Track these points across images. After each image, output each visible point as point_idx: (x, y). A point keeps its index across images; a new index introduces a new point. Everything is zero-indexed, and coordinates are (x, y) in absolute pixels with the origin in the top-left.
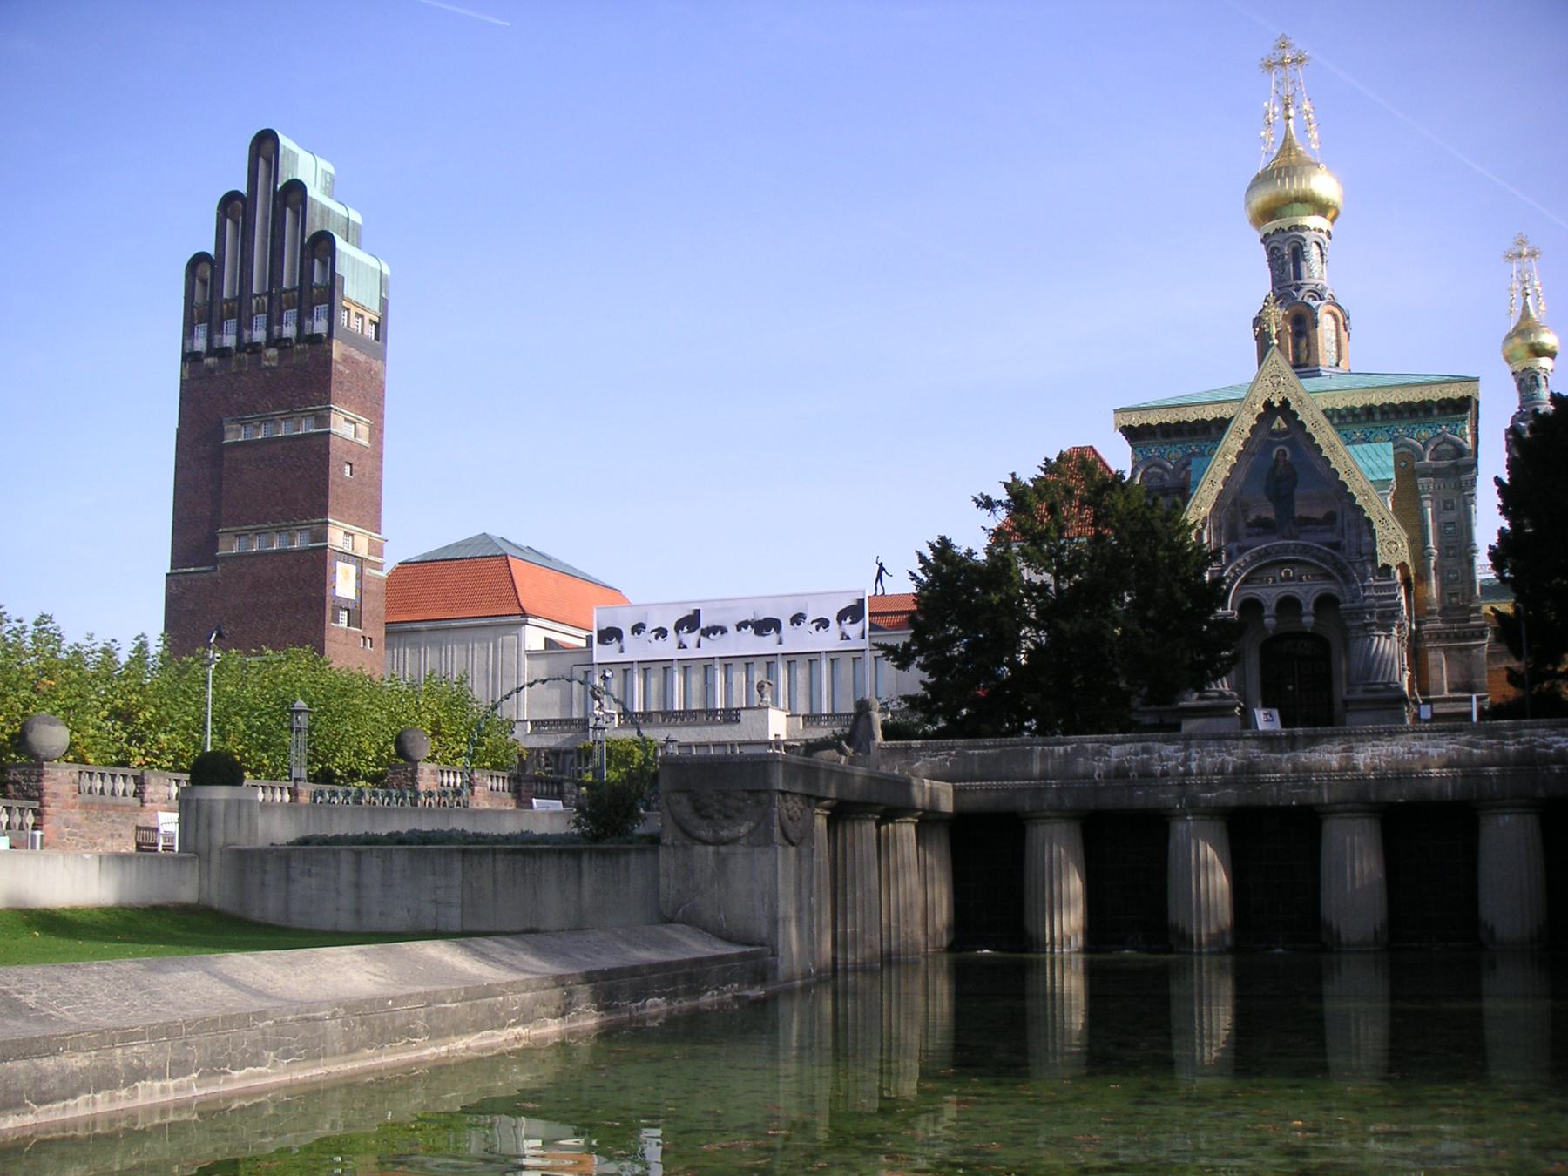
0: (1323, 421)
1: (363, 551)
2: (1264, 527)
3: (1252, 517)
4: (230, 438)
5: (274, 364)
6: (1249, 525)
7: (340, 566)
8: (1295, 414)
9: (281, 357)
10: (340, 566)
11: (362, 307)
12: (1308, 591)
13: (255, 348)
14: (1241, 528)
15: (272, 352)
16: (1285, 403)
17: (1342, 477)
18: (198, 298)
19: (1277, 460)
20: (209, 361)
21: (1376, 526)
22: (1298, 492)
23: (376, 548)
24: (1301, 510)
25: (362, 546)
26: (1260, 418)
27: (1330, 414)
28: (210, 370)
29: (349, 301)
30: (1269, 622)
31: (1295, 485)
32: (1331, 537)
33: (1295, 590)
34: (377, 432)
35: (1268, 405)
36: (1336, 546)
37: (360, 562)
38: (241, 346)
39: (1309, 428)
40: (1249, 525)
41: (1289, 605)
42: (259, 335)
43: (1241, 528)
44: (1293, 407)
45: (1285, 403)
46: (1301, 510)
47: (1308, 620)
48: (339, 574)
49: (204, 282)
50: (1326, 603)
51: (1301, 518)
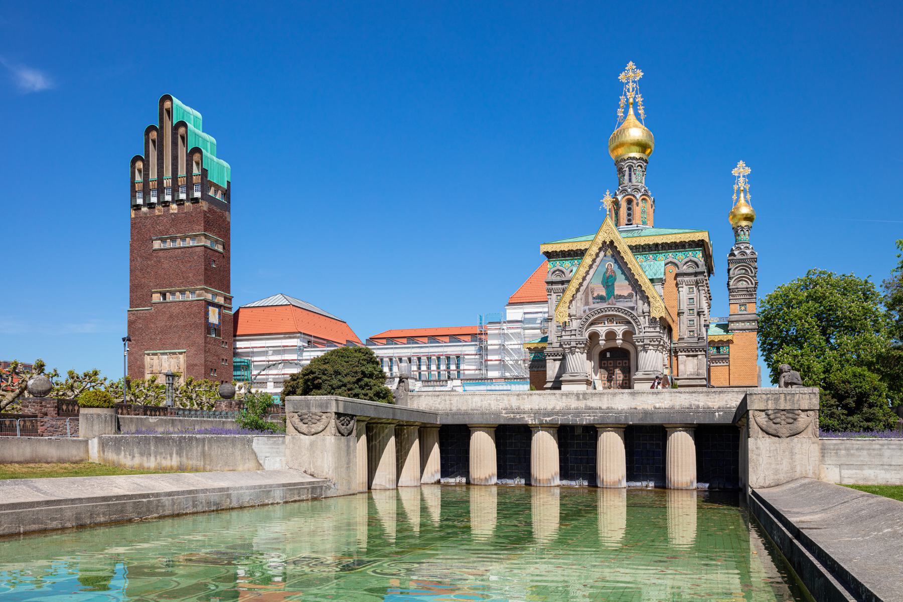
0: (629, 251)
2: (601, 299)
3: (595, 295)
5: (176, 211)
6: (594, 298)
7: (211, 308)
8: (616, 247)
12: (620, 329)
13: (166, 204)
14: (591, 300)
16: (612, 242)
17: (636, 277)
18: (138, 178)
19: (607, 269)
21: (651, 300)
22: (616, 284)
23: (228, 299)
24: (616, 292)
25: (220, 300)
26: (600, 249)
27: (631, 247)
30: (602, 342)
32: (632, 305)
35: (604, 242)
36: (632, 308)
37: (219, 306)
38: (159, 203)
39: (622, 254)
40: (594, 298)
41: (611, 335)
43: (591, 300)
44: (615, 244)
45: (612, 242)
46: (616, 292)
47: (619, 342)
48: (210, 313)
49: (140, 171)
50: (628, 335)
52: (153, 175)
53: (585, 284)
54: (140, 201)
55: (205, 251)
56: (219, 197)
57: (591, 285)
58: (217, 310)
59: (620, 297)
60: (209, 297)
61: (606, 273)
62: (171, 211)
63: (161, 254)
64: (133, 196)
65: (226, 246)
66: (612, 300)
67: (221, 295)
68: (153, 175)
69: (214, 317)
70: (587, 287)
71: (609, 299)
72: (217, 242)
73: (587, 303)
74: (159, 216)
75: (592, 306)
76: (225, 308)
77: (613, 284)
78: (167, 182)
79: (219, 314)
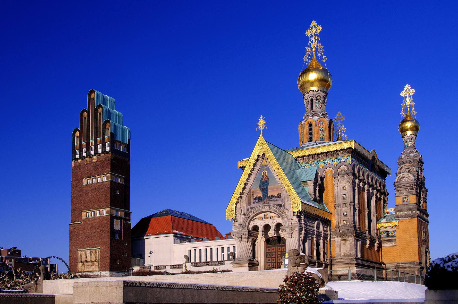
1: (123, 216)
2: (259, 199)
3: (255, 196)
6: (254, 199)
7: (115, 220)
9: (97, 159)
10: (115, 220)
11: (121, 142)
14: (252, 201)
15: (95, 157)
19: (263, 176)
20: (80, 161)
24: (270, 194)
28: (79, 164)
31: (268, 184)
32: (280, 202)
33: (268, 222)
36: (280, 205)
40: (254, 199)
42: (92, 153)
43: (252, 201)
46: (270, 194)
48: (115, 223)
51: (270, 196)
58: (119, 221)
59: (272, 197)
61: (262, 179)
62: (93, 161)
64: (74, 154)
65: (127, 180)
66: (267, 200)
67: (122, 211)
70: (249, 191)
71: (264, 199)
73: (249, 204)
74: (86, 164)
75: (253, 205)
77: (267, 188)
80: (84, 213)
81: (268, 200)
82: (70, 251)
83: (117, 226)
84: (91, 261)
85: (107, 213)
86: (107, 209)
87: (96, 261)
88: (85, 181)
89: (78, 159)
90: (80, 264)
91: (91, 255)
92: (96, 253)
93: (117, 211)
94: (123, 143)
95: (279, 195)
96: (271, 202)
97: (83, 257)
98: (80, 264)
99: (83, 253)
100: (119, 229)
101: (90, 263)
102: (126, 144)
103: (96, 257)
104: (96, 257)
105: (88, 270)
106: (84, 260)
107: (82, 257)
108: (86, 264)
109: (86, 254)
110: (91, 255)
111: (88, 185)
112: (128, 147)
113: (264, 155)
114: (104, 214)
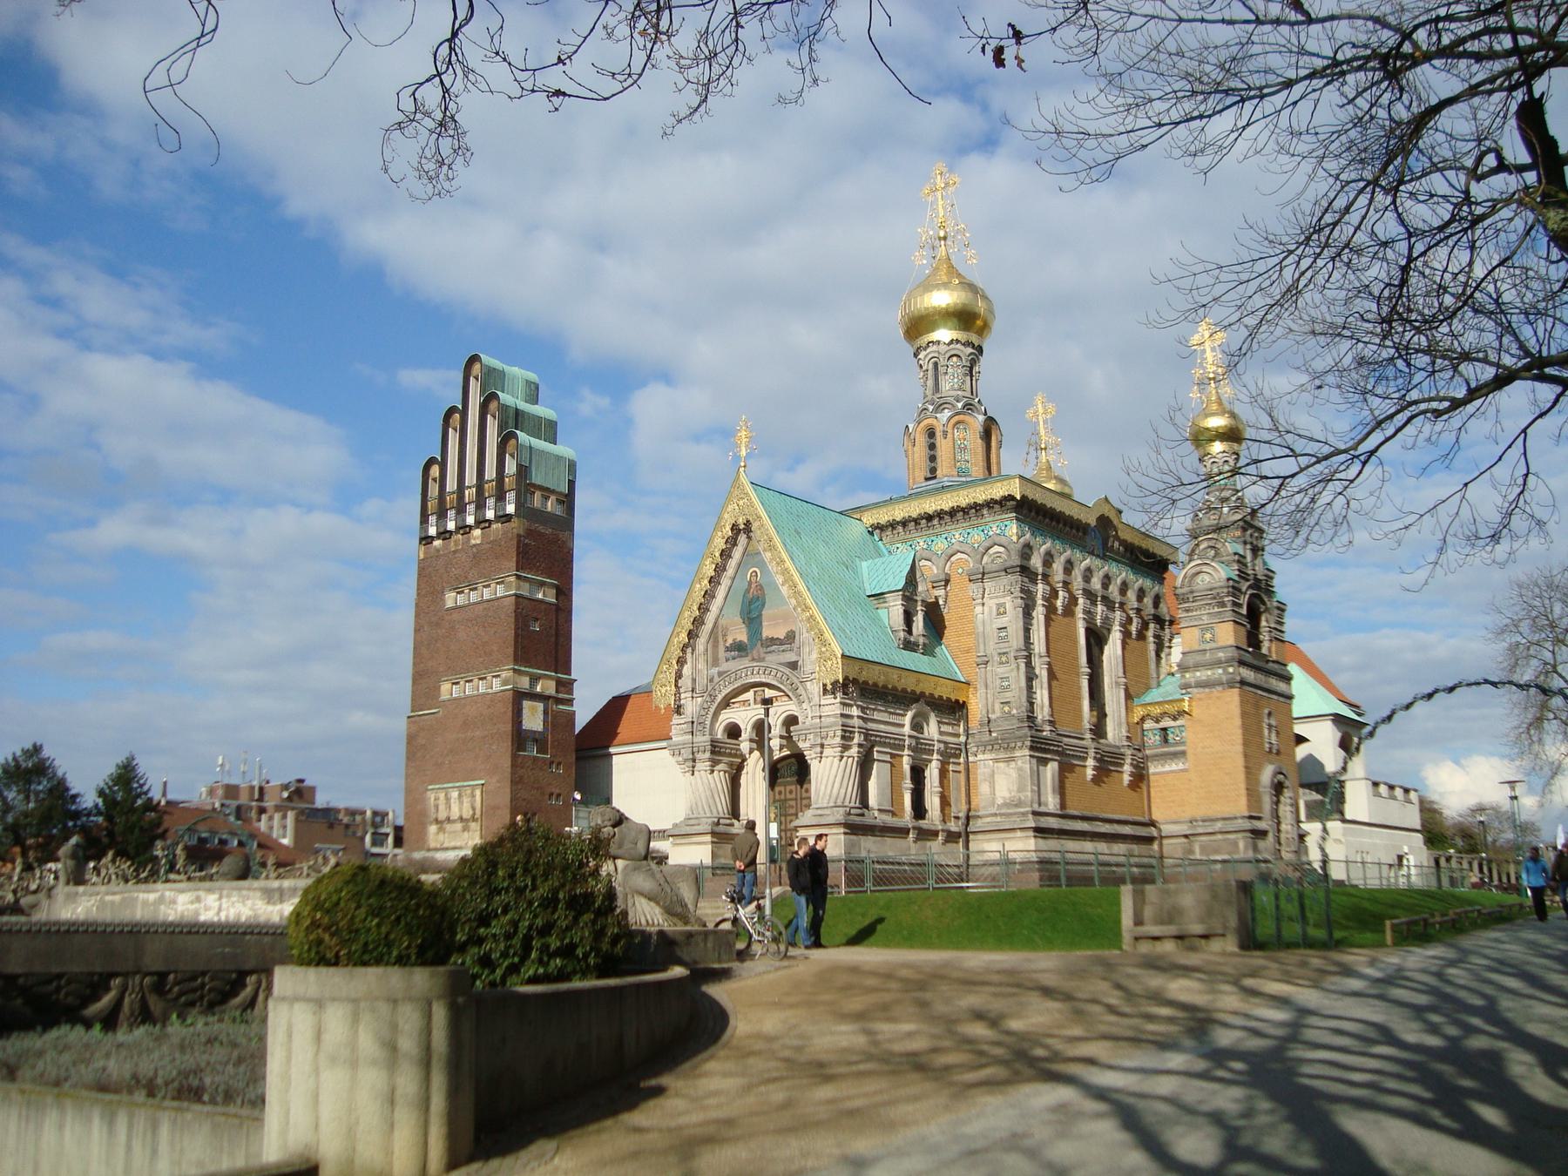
2: (739, 648)
3: (730, 641)
4: (450, 604)
6: (728, 649)
7: (526, 704)
10: (526, 704)
11: (547, 490)
14: (722, 653)
15: (477, 532)
19: (750, 583)
23: (566, 686)
24: (767, 632)
25: (546, 686)
29: (534, 486)
32: (791, 657)
34: (564, 592)
35: (734, 527)
36: (793, 666)
40: (728, 649)
42: (470, 520)
43: (722, 653)
46: (767, 632)
48: (526, 712)
52: (451, 484)
53: (710, 619)
54: (432, 531)
55: (517, 604)
56: (551, 506)
57: (722, 622)
58: (540, 706)
59: (773, 641)
60: (524, 683)
61: (748, 591)
63: (455, 616)
66: (759, 650)
67: (550, 677)
68: (451, 484)
69: (533, 719)
72: (542, 584)
75: (724, 666)
76: (559, 701)
77: (760, 616)
78: (470, 494)
79: (545, 712)
80: (445, 687)
81: (762, 650)
82: (408, 791)
83: (533, 719)
84: (461, 819)
85: (505, 683)
86: (504, 674)
87: (474, 819)
88: (451, 599)
89: (432, 538)
90: (433, 829)
91: (461, 803)
92: (473, 796)
93: (534, 679)
94: (553, 492)
95: (791, 637)
96: (769, 658)
97: (442, 807)
98: (433, 829)
99: (442, 796)
100: (540, 728)
101: (459, 826)
102: (560, 494)
103: (474, 809)
104: (474, 809)
105: (453, 844)
106: (442, 815)
107: (437, 807)
108: (448, 827)
109: (448, 799)
110: (461, 803)
111: (456, 608)
112: (568, 500)
113: (748, 524)
114: (497, 686)
